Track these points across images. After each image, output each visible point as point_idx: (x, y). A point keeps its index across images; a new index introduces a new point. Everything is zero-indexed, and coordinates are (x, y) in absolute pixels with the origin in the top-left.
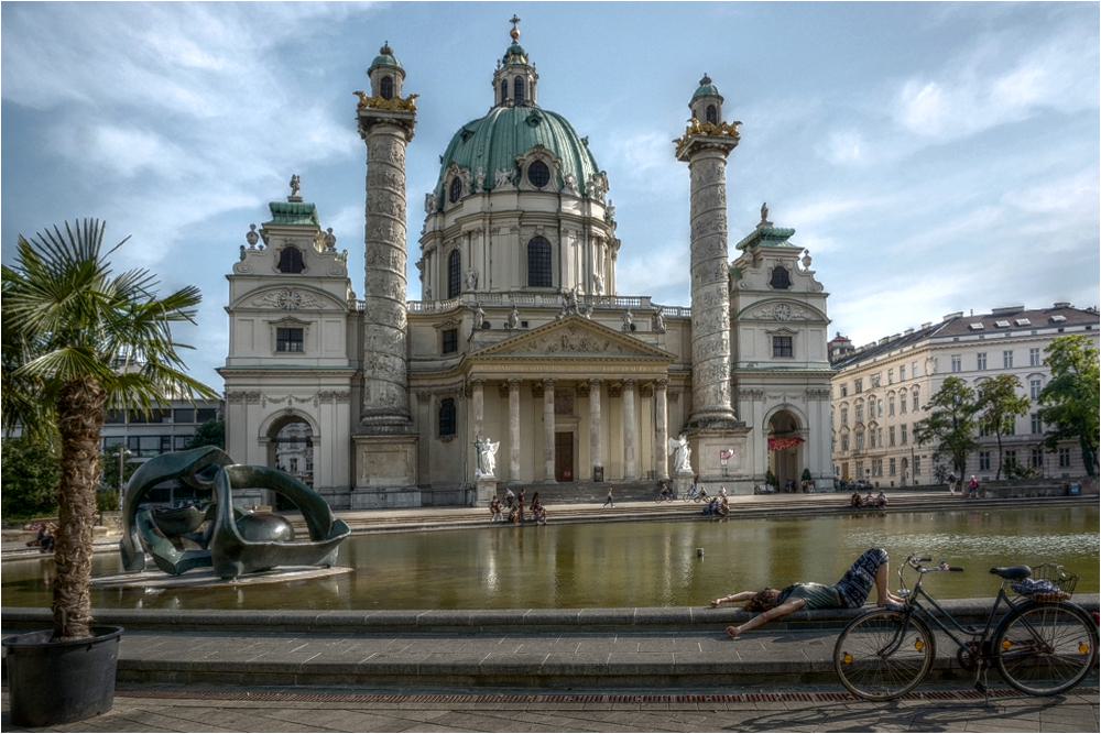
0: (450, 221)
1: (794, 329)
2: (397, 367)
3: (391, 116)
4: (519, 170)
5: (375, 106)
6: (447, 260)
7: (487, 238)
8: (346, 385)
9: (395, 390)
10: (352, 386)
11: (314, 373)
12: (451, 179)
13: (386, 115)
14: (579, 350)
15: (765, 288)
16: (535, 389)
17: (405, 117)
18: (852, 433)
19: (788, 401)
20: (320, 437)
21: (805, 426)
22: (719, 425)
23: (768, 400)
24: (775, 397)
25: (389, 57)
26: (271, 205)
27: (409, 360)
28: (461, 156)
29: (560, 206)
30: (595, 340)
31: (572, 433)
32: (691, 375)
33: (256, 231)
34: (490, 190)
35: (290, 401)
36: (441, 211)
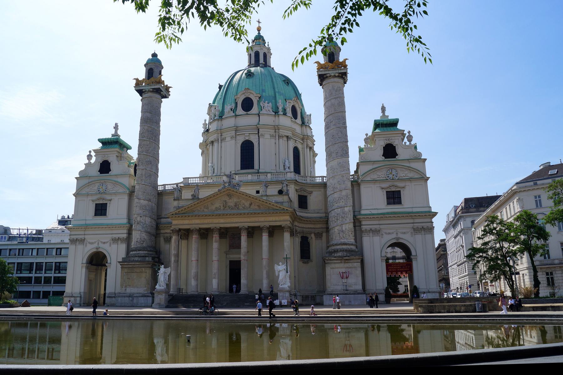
1: (400, 184)
2: (147, 223)
3: (149, 87)
4: (236, 104)
7: (219, 144)
9: (144, 235)
17: (157, 86)
19: (400, 236)
20: (111, 263)
22: (340, 254)
23: (385, 235)
24: (389, 233)
26: (99, 140)
27: (159, 217)
29: (259, 121)
30: (243, 201)
32: (328, 219)
33: (91, 154)
34: (222, 117)
35: (98, 243)
36: (208, 130)
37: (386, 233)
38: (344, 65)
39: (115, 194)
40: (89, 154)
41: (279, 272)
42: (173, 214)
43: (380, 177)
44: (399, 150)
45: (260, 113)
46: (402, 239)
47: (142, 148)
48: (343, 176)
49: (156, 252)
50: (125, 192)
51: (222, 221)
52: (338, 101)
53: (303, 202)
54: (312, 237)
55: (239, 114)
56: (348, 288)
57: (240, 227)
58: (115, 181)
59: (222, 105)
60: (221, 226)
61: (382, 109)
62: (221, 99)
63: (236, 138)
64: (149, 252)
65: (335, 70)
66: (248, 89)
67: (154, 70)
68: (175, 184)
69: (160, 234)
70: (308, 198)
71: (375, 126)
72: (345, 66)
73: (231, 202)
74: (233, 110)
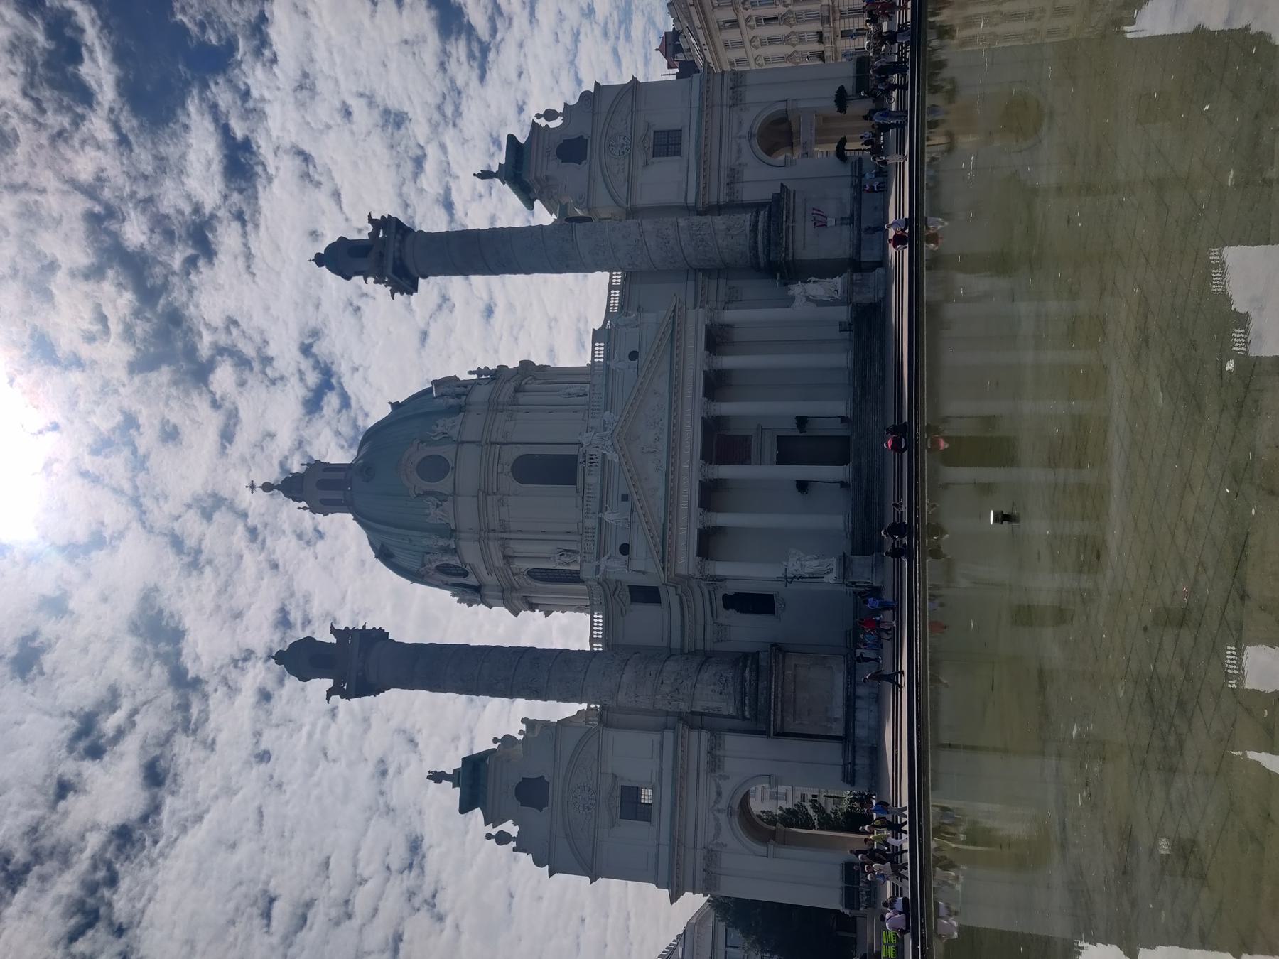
0: (491, 579)
4: (427, 493)
6: (540, 585)
7: (513, 536)
9: (707, 675)
10: (702, 728)
15: (585, 165)
16: (711, 494)
18: (799, 28)
21: (782, 106)
24: (739, 151)
28: (411, 563)
29: (473, 442)
31: (778, 436)
32: (700, 270)
33: (494, 834)
35: (719, 811)
37: (739, 158)
40: (493, 841)
41: (808, 298)
42: (663, 568)
44: (573, 133)
45: (455, 439)
46: (751, 128)
50: (599, 738)
56: (848, 214)
60: (699, 457)
61: (483, 178)
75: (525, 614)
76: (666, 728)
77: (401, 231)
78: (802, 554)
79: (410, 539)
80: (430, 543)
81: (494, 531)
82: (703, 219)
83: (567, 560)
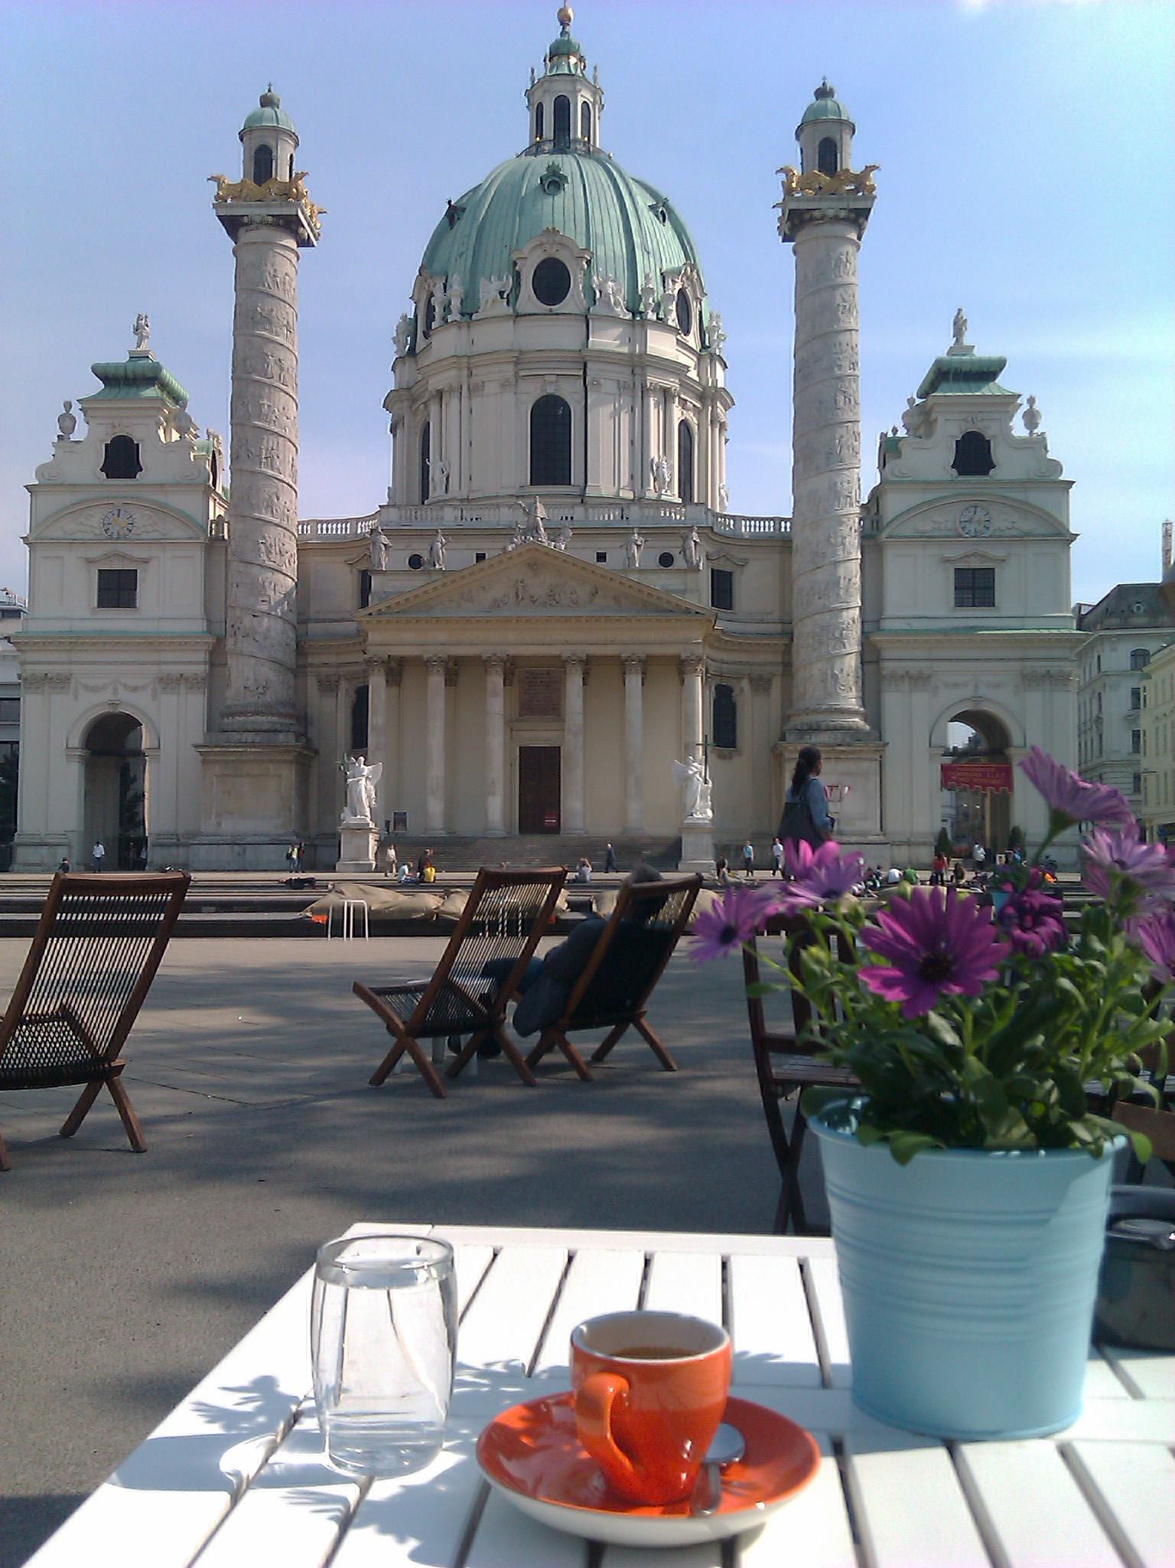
1: (997, 552)
3: (264, 211)
4: (517, 277)
5: (240, 197)
8: (198, 663)
9: (268, 672)
10: (212, 664)
11: (151, 642)
12: (424, 297)
13: (257, 211)
14: (544, 604)
17: (285, 211)
19: (983, 691)
24: (956, 685)
25: (268, 110)
36: (412, 352)
38: (861, 182)
39: (160, 542)
42: (370, 614)
43: (942, 526)
44: (998, 453)
47: (248, 405)
48: (841, 523)
49: (298, 718)
51: (512, 637)
52: (842, 296)
53: (722, 588)
54: (742, 689)
55: (524, 312)
57: (564, 656)
58: (160, 504)
59: (468, 277)
61: (955, 323)
62: (461, 255)
63: (516, 386)
64: (282, 720)
65: (839, 200)
66: (555, 232)
67: (274, 154)
68: (346, 521)
69: (305, 666)
70: (736, 578)
71: (932, 376)
72: (869, 193)
73: (538, 587)
74: (508, 295)
75: (388, 418)
76: (209, 621)
77: (853, 216)
78: (375, 781)
79: (462, 254)
80: (456, 287)
81: (470, 375)
82: (853, 646)
83: (437, 479)
